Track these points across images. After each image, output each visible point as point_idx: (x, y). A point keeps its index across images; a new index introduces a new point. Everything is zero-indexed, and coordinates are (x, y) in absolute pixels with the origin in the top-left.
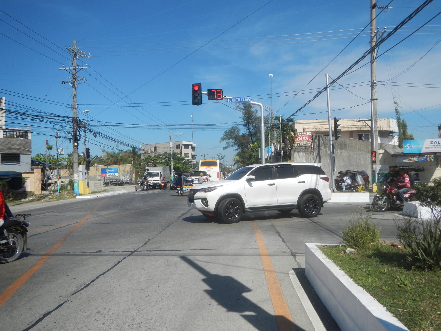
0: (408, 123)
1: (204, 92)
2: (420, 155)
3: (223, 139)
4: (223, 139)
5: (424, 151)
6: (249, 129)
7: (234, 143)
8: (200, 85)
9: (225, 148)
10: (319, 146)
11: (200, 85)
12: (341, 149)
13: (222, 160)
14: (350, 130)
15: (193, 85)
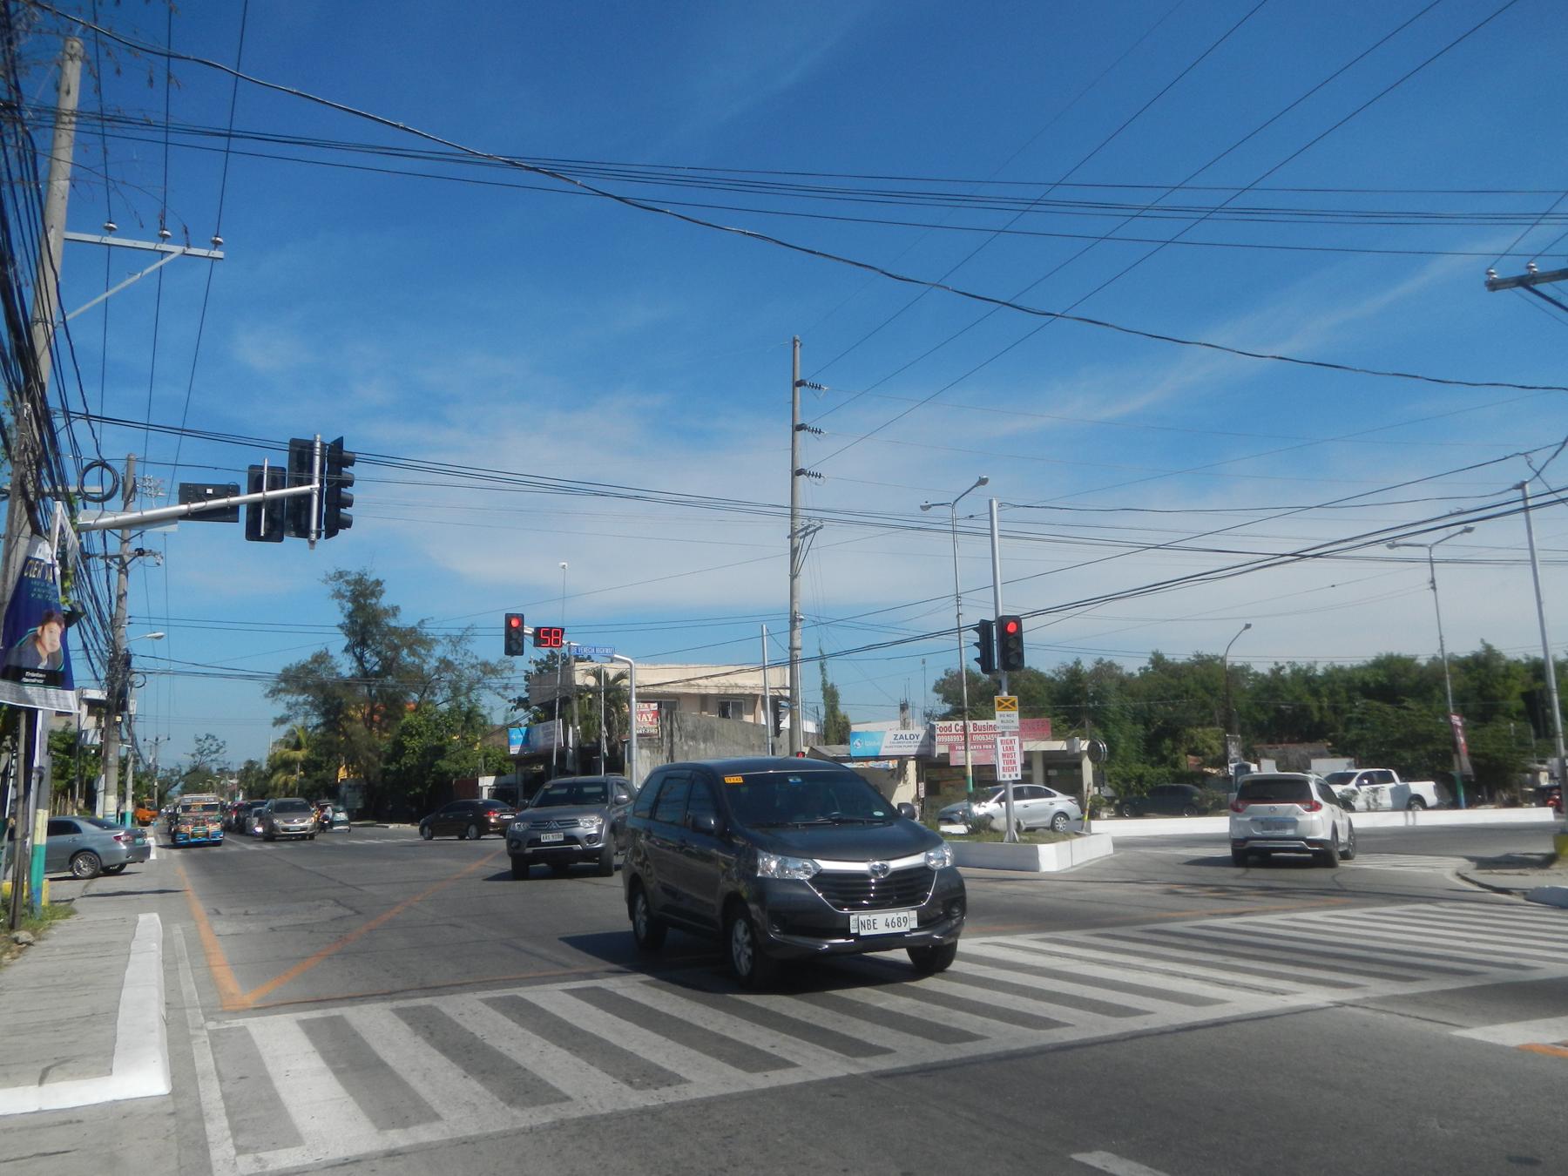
0: (840, 690)
1: (528, 630)
2: (877, 758)
3: (274, 692)
4: (274, 692)
5: (884, 752)
6: (360, 659)
7: (312, 704)
8: (520, 618)
9: (281, 721)
10: (671, 735)
11: (520, 618)
12: (705, 741)
13: (213, 756)
14: (703, 691)
15: (509, 618)
